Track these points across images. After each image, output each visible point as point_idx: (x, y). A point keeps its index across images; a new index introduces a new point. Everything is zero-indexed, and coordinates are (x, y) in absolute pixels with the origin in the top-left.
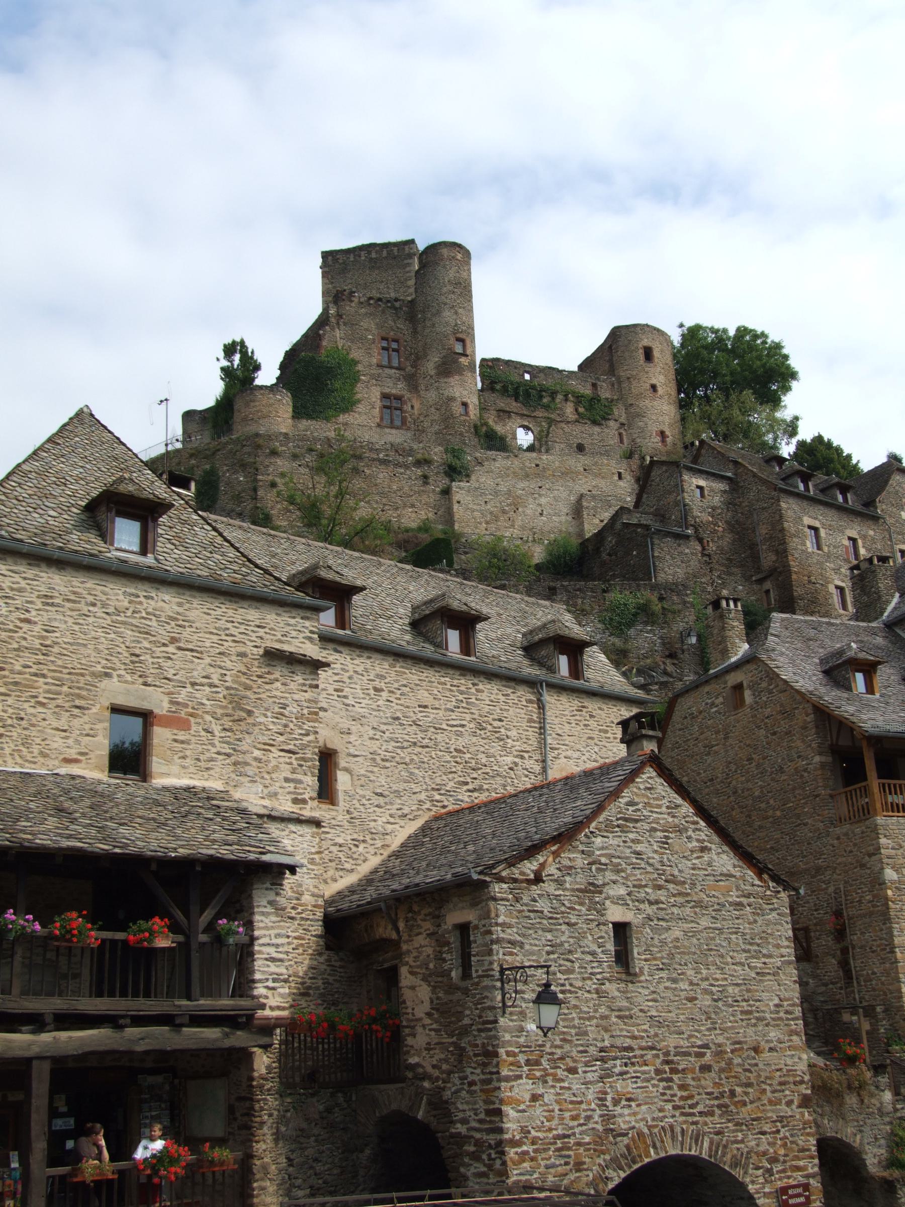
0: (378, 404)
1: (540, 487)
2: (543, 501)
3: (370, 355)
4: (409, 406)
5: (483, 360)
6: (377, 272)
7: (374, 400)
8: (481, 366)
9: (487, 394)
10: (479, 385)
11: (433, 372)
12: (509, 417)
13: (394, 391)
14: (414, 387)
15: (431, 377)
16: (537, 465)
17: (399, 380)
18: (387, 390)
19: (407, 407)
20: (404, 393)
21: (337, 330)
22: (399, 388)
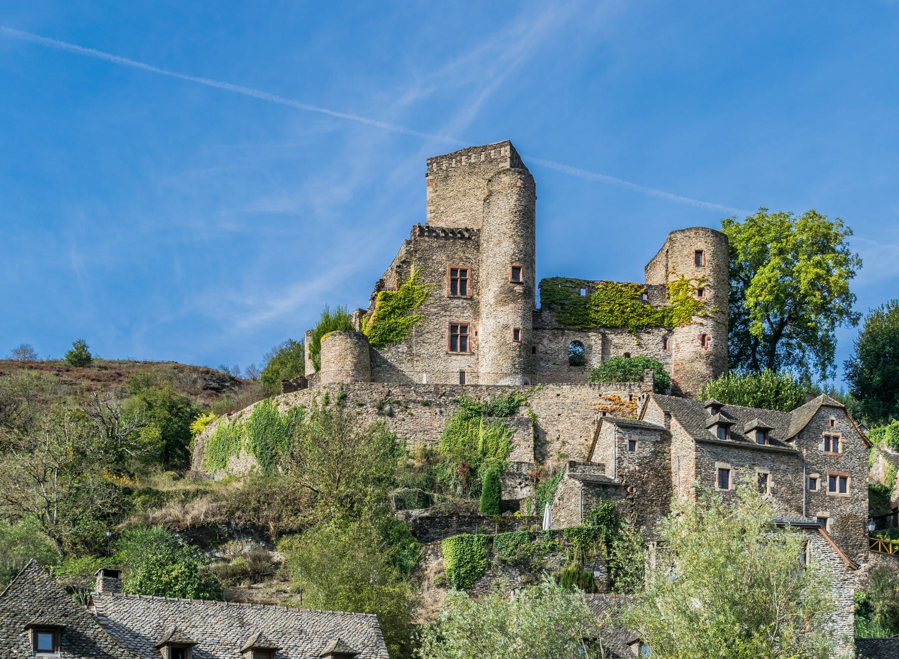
0: (447, 334)
1: (559, 415)
2: (560, 427)
3: (440, 287)
4: (474, 332)
5: (544, 282)
6: (475, 177)
7: (443, 330)
8: (540, 286)
9: (546, 314)
10: (538, 306)
11: (492, 301)
12: (563, 334)
13: (461, 320)
14: (477, 314)
15: (491, 305)
16: (558, 395)
17: (464, 308)
18: (455, 320)
19: (470, 334)
20: (470, 320)
21: (412, 266)
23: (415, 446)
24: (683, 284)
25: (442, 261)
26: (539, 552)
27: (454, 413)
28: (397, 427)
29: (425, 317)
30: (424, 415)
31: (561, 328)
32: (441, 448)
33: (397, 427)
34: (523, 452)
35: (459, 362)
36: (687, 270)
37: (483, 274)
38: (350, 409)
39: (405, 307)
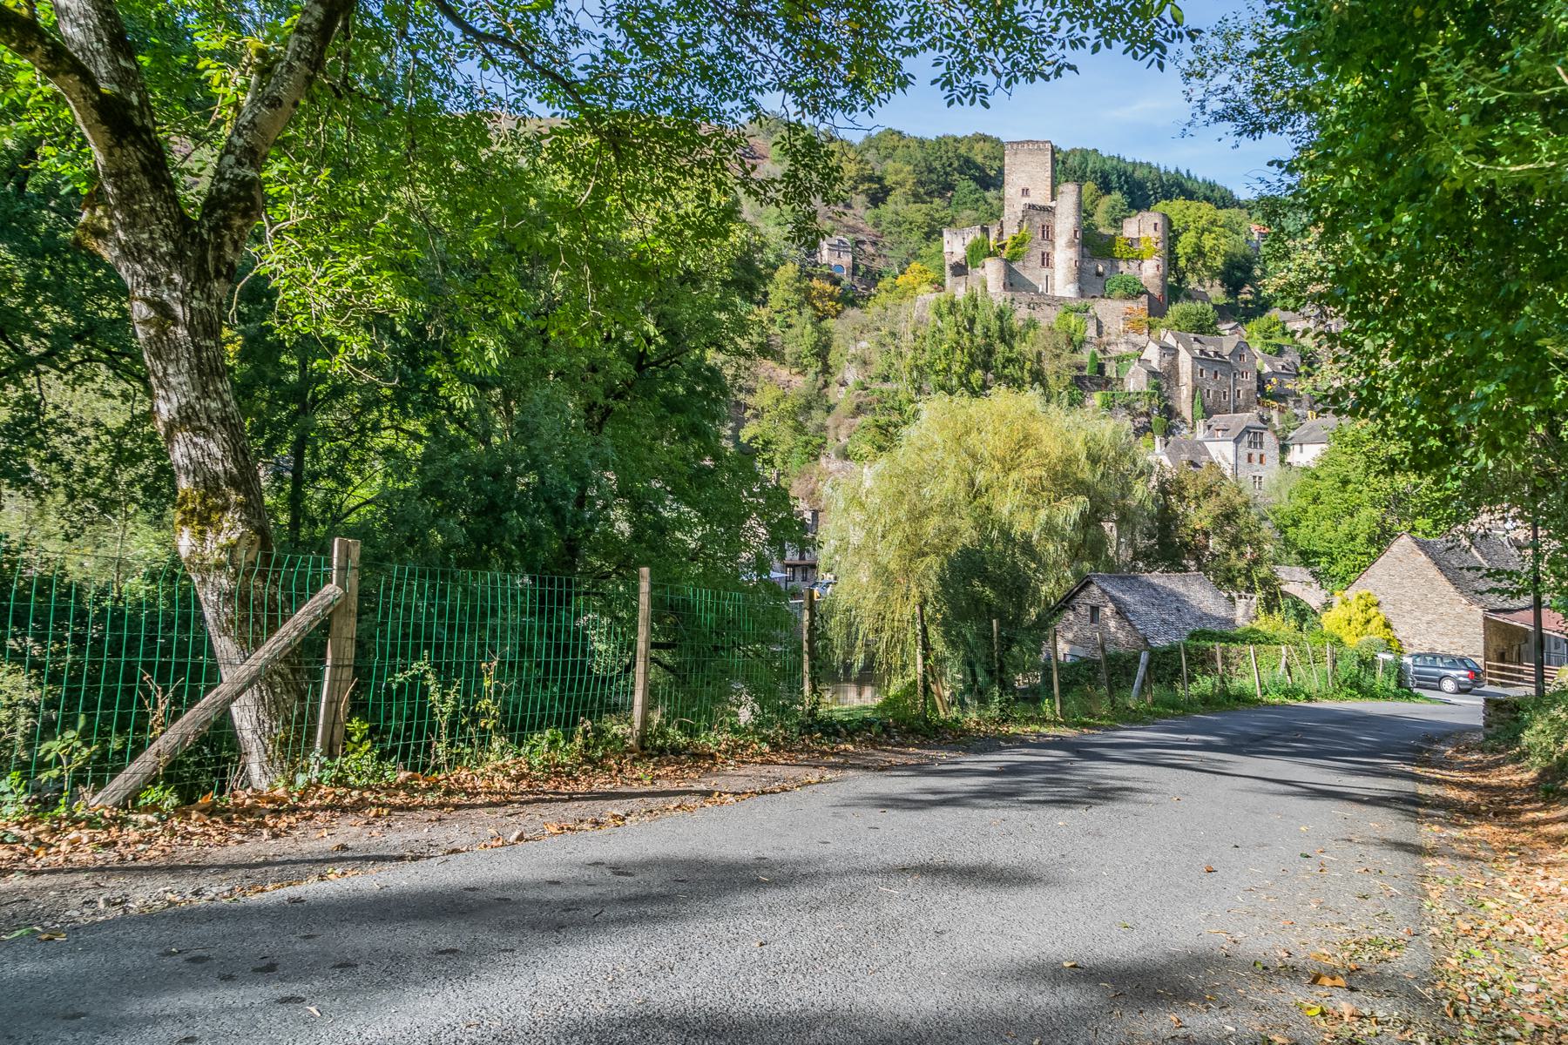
22: (1049, 249)
23: (1043, 324)
24: (1148, 239)
25: (1038, 220)
26: (1132, 401)
27: (1062, 310)
28: (1037, 315)
29: (1031, 248)
30: (1048, 310)
31: (1093, 257)
32: (1055, 326)
33: (1037, 315)
34: (1092, 332)
35: (1046, 271)
36: (1151, 233)
37: (1057, 230)
38: (1016, 305)
39: (1022, 244)
